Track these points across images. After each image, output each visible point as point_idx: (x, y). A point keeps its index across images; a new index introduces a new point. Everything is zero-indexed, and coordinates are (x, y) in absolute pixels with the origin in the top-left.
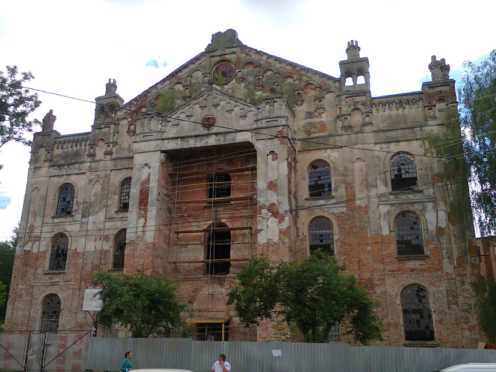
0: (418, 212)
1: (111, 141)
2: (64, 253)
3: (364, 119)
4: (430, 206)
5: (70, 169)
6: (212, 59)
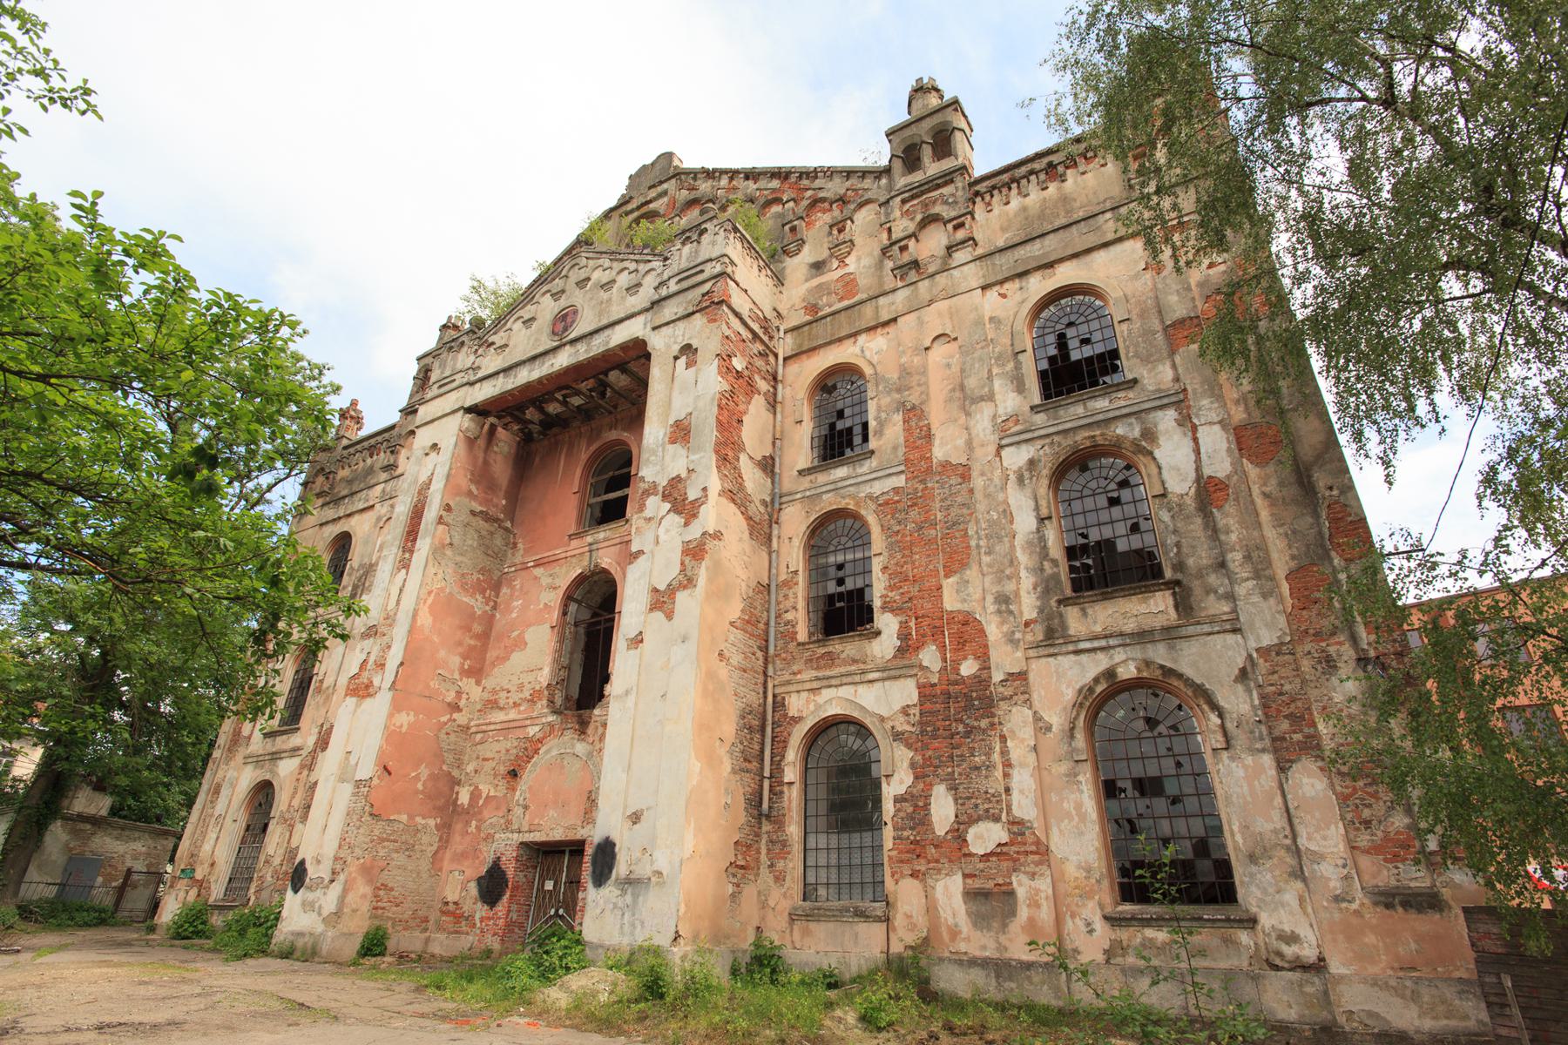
4: (1166, 420)
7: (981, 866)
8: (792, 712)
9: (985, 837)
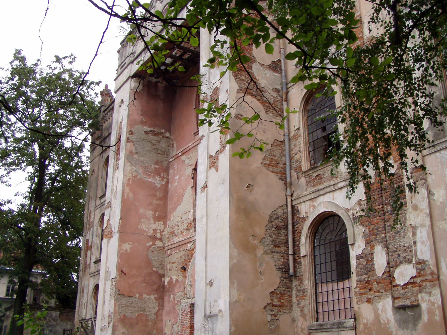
7: (403, 291)
9: (404, 274)
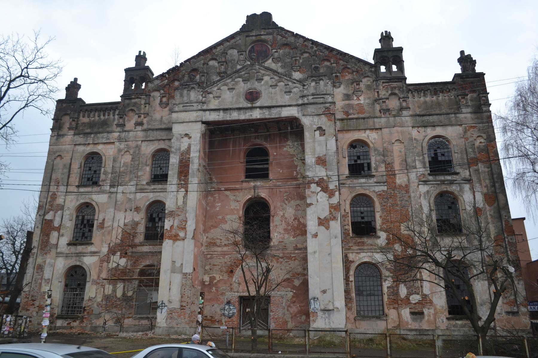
0: (456, 193)
1: (142, 112)
2: (90, 223)
3: (400, 103)
5: (98, 138)
6: (247, 38)
8: (351, 259)
9: (415, 298)
